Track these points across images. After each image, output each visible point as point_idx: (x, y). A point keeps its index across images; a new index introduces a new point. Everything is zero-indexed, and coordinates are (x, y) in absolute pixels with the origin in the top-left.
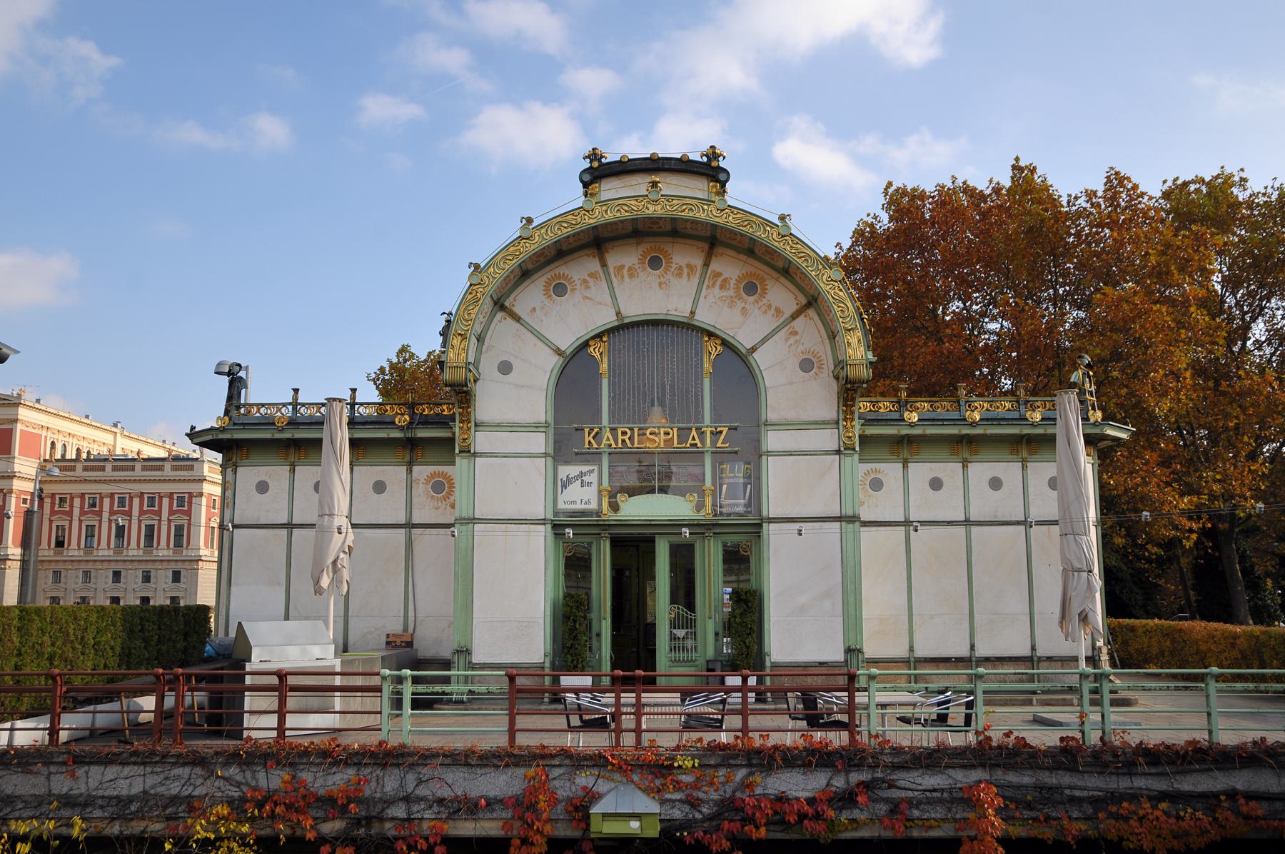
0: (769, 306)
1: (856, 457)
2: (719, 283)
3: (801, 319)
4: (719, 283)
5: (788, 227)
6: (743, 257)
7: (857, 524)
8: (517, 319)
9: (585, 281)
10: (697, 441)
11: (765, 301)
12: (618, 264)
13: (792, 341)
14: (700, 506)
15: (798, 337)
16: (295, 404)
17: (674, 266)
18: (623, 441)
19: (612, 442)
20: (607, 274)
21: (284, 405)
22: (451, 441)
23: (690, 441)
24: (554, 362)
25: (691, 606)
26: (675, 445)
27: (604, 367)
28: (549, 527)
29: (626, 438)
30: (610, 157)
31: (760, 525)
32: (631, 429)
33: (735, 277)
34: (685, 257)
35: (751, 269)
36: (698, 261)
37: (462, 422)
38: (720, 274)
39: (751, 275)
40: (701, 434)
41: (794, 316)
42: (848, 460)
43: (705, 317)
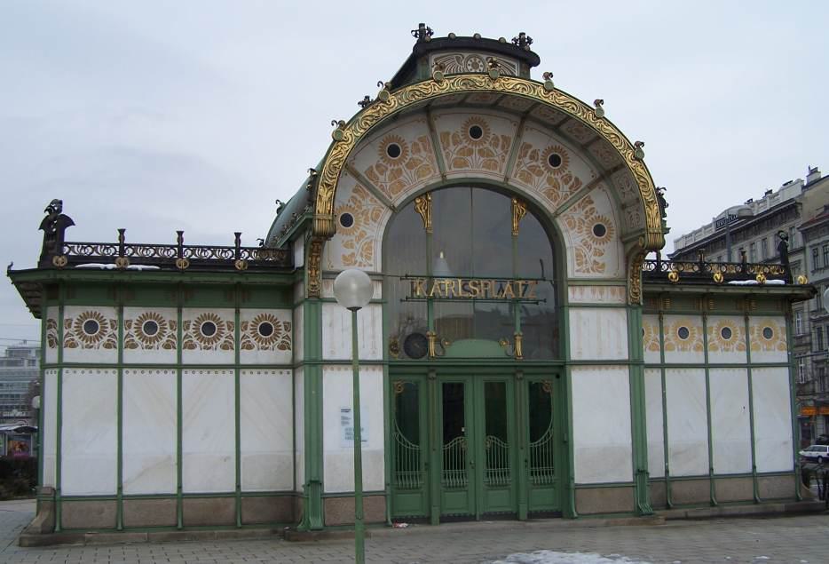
0: (570, 177)
1: (640, 310)
3: (596, 190)
5: (602, 111)
6: (550, 132)
7: (642, 366)
9: (415, 144)
11: (566, 172)
12: (446, 130)
13: (587, 209)
15: (593, 206)
16: (122, 245)
20: (434, 139)
21: (112, 245)
24: (386, 215)
25: (504, 437)
28: (387, 366)
30: (439, 32)
33: (542, 149)
34: (499, 128)
37: (310, 269)
38: (530, 146)
39: (556, 149)
41: (590, 187)
43: (517, 183)
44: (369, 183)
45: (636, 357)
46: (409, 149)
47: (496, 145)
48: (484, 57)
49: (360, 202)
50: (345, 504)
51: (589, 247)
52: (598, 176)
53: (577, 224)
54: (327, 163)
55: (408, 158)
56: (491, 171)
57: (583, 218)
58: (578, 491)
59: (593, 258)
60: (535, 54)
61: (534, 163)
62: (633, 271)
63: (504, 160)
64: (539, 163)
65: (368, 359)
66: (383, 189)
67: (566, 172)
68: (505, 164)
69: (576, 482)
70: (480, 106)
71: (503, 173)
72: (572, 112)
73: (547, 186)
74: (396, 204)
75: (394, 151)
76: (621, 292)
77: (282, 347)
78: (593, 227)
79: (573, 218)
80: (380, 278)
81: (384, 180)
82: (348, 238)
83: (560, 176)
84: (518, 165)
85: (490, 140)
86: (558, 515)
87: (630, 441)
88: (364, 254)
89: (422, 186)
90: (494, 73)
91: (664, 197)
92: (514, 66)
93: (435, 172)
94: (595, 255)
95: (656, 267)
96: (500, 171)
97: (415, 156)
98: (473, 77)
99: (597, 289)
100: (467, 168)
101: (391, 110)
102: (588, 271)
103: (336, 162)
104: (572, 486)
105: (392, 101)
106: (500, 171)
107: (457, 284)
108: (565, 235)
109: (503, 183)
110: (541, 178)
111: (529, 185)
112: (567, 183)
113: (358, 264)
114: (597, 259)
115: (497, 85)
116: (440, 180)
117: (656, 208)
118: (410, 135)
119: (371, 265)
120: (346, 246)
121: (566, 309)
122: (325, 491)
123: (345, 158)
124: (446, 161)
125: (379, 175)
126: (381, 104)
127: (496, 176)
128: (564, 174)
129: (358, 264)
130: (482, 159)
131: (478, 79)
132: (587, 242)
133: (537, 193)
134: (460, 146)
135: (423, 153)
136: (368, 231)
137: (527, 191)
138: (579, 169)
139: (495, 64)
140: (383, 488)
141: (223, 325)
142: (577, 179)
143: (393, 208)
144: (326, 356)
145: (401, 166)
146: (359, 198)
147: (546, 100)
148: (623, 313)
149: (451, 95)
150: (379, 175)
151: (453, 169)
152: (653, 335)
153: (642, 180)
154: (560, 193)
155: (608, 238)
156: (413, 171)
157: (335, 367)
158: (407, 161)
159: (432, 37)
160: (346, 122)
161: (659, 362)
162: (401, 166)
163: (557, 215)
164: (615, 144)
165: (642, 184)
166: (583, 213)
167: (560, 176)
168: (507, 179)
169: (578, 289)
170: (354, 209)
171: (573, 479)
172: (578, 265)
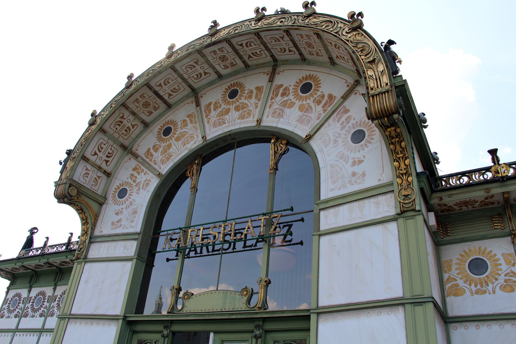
2: (281, 92)
4: (281, 92)
12: (207, 103)
13: (343, 119)
24: (155, 182)
35: (304, 74)
41: (345, 97)
42: (410, 222)
43: (270, 122)
45: (417, 291)
47: (250, 97)
53: (332, 138)
56: (245, 120)
59: (351, 169)
61: (286, 98)
64: (291, 97)
65: (107, 313)
66: (155, 164)
67: (319, 93)
68: (258, 110)
72: (281, 24)
74: (164, 173)
80: (137, 237)
81: (158, 156)
82: (121, 207)
83: (312, 99)
88: (129, 218)
89: (187, 151)
93: (198, 137)
94: (354, 164)
96: (253, 118)
100: (224, 125)
102: (344, 186)
108: (319, 155)
109: (254, 127)
111: (281, 119)
112: (319, 102)
114: (356, 169)
119: (132, 227)
120: (117, 214)
124: (207, 126)
128: (315, 96)
134: (220, 110)
135: (190, 126)
137: (280, 126)
138: (332, 85)
142: (331, 97)
148: (393, 226)
151: (213, 130)
152: (504, 267)
156: (180, 142)
157: (79, 321)
163: (309, 137)
166: (339, 125)
167: (312, 99)
168: (259, 121)
169: (331, 211)
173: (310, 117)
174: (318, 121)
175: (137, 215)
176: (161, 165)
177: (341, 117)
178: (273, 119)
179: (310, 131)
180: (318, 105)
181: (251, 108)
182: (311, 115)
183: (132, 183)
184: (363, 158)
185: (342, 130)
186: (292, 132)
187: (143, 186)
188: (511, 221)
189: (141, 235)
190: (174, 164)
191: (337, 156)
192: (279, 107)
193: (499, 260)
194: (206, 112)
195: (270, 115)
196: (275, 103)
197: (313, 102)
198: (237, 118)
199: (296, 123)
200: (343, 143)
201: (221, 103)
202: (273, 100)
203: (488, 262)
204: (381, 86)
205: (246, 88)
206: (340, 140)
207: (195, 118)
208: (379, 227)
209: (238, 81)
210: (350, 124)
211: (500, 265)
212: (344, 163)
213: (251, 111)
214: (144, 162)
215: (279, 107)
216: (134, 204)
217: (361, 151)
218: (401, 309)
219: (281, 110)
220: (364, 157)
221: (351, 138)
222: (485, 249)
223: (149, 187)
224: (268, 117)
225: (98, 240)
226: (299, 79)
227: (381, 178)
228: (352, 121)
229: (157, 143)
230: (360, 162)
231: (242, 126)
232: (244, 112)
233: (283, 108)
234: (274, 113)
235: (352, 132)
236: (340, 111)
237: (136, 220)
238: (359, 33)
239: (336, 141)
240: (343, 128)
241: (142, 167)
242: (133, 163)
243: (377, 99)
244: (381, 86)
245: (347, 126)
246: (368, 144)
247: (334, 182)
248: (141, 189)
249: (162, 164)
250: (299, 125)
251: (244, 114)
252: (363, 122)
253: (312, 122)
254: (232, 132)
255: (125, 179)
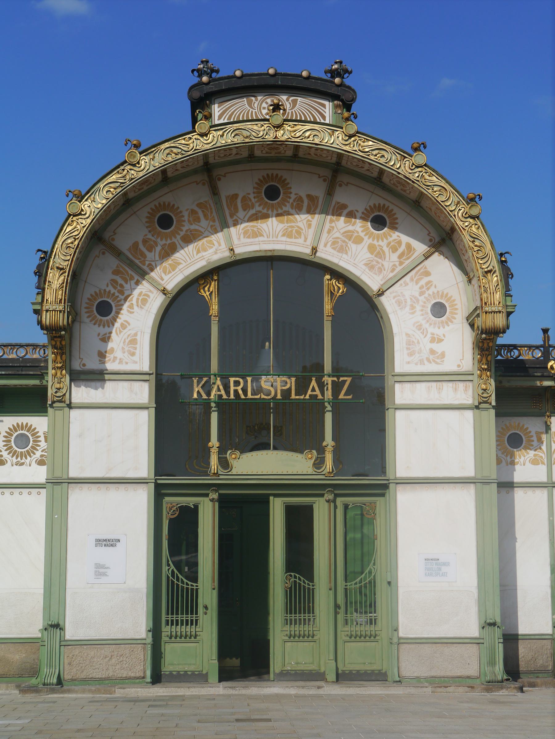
1: (493, 412)
8: (118, 253)
9: (193, 212)
10: (318, 392)
13: (423, 282)
14: (319, 463)
17: (293, 196)
18: (236, 391)
19: (223, 392)
20: (218, 203)
22: (42, 392)
23: (309, 392)
25: (309, 575)
26: (293, 396)
27: (214, 308)
29: (239, 388)
31: (386, 487)
32: (244, 377)
36: (319, 192)
38: (344, 207)
39: (379, 208)
40: (322, 386)
43: (328, 254)
44: (132, 261)
46: (186, 218)
48: (284, 97)
49: (122, 286)
50: (93, 653)
51: (424, 333)
52: (437, 239)
53: (409, 302)
54: (60, 242)
55: (184, 229)
56: (293, 240)
57: (417, 294)
58: (403, 647)
59: (430, 346)
60: (349, 87)
61: (350, 228)
62: (480, 361)
63: (309, 226)
68: (311, 232)
69: (401, 634)
70: (278, 160)
71: (309, 242)
72: (382, 161)
73: (369, 255)
75: (165, 222)
76: (466, 390)
77: (41, 463)
78: (429, 306)
79: (404, 296)
84: (329, 232)
85: (291, 201)
86: (378, 677)
87: (476, 584)
88: (126, 349)
90: (278, 118)
91: (509, 264)
92: (324, 106)
93: (220, 245)
94: (433, 340)
95: (543, 354)
96: (305, 241)
97: (193, 227)
98: (248, 125)
99: (434, 384)
100: (261, 239)
101: (141, 174)
102: (422, 362)
103: (69, 241)
104: (395, 640)
105: (143, 162)
106: (305, 241)
107: (246, 382)
108: (392, 317)
110: (360, 246)
111: (344, 256)
112: (394, 250)
113: (118, 361)
114: (435, 346)
115: (280, 133)
116: (227, 254)
117: (495, 278)
118: (186, 200)
121: (389, 414)
122: (68, 637)
123: (81, 235)
125: (147, 253)
126: (129, 167)
127: (299, 247)
128: (391, 239)
129: (118, 361)
130: (281, 226)
131: (255, 127)
132: (421, 325)
133: (355, 265)
135: (204, 223)
136: (130, 320)
137: (343, 264)
139: (276, 107)
140: (144, 636)
141: (39, 437)
143: (164, 291)
144: (73, 473)
145: (174, 240)
146: (120, 281)
147: (345, 148)
148: (469, 415)
149: (227, 149)
150: (147, 253)
151: (244, 240)
153: (477, 243)
154: (386, 264)
155: (450, 320)
158: (182, 233)
159: (220, 75)
160: (83, 194)
161: (544, 479)
162: (174, 240)
164: (439, 199)
165: (476, 249)
168: (314, 250)
169: (407, 386)
170: (114, 294)
171: (396, 630)
172: (411, 354)
173: (383, 265)
174: (391, 275)
175: (138, 346)
176: (163, 275)
177: (421, 279)
178: (333, 251)
179: (382, 283)
180: (393, 252)
181: (300, 224)
182: (383, 263)
183: (117, 294)
184: (443, 338)
185: (420, 296)
186: (358, 278)
187: (137, 302)
188: (548, 403)
189: (154, 376)
190: (186, 277)
191: (414, 325)
192: (341, 236)
193: (532, 436)
194: (229, 209)
195: (329, 244)
196: (335, 230)
197: (387, 247)
198: (280, 234)
199: (364, 267)
200: (421, 313)
201: (253, 200)
202: (333, 224)
203: (523, 437)
204: (494, 304)
205: (292, 190)
206: (418, 308)
207: (212, 213)
208: (456, 413)
209: (280, 173)
210: (430, 292)
211: (533, 441)
212: (421, 335)
213: (302, 230)
214: (132, 265)
215: (341, 236)
216: (129, 328)
217: (441, 328)
218: (472, 485)
219: (344, 241)
220: (444, 336)
221: (431, 311)
222: (523, 425)
223: (147, 305)
224: (325, 245)
225: (82, 377)
226: (370, 206)
227: (461, 364)
228: (432, 289)
229: (150, 236)
230: (440, 341)
231: (289, 248)
232: (290, 227)
233: (347, 241)
234: (334, 243)
235: (433, 302)
236: (419, 270)
237: (137, 352)
238: (476, 224)
239: (412, 307)
240: (422, 294)
241: (130, 272)
242: (112, 262)
243: (490, 316)
244: (494, 304)
245: (427, 293)
246: (450, 323)
247: (411, 354)
248: (135, 307)
249: (165, 273)
250: (367, 270)
251: (292, 231)
252: (445, 293)
253: (385, 272)
254: (276, 254)
255: (103, 287)
